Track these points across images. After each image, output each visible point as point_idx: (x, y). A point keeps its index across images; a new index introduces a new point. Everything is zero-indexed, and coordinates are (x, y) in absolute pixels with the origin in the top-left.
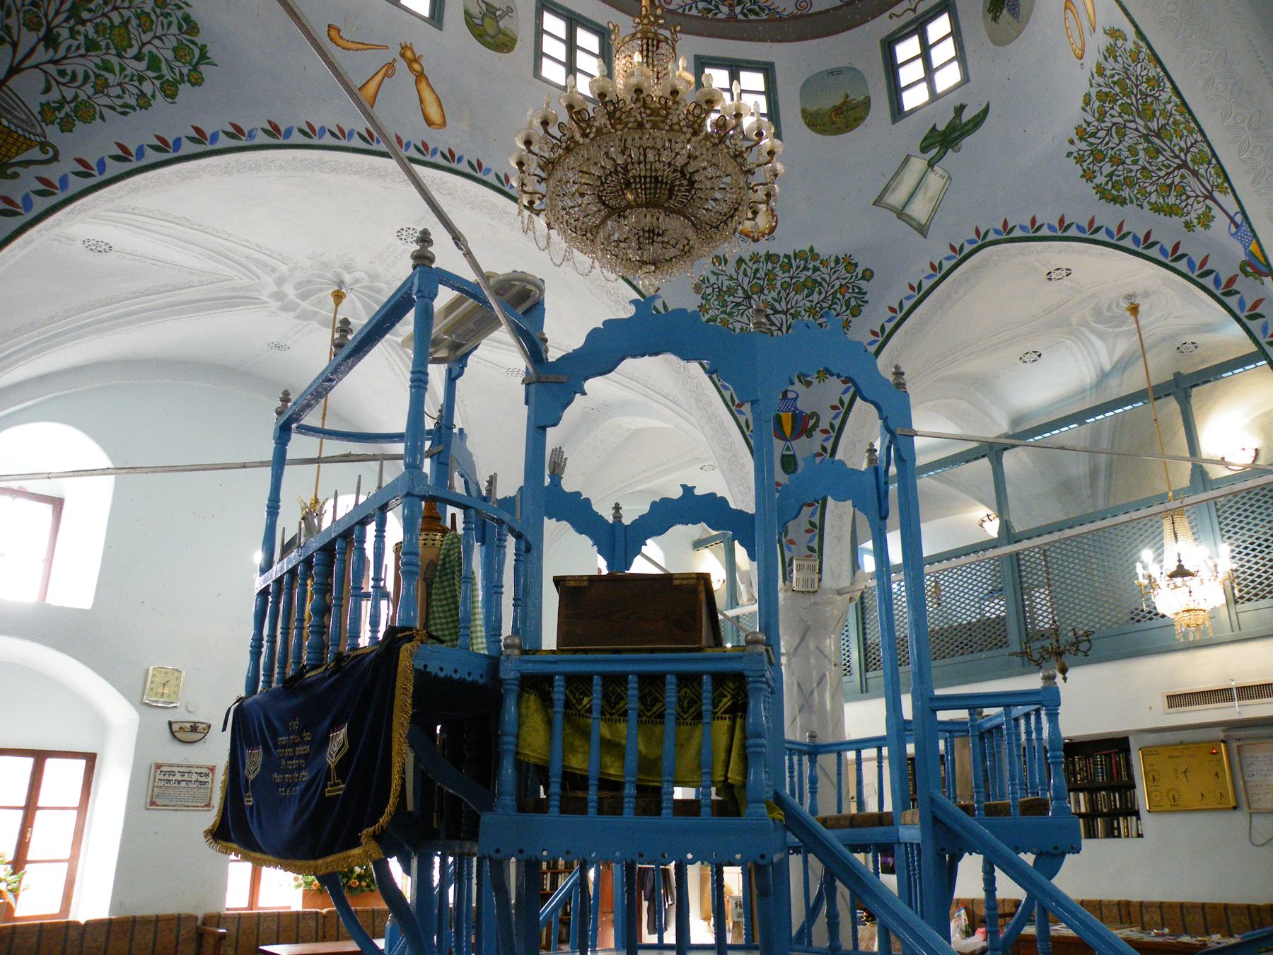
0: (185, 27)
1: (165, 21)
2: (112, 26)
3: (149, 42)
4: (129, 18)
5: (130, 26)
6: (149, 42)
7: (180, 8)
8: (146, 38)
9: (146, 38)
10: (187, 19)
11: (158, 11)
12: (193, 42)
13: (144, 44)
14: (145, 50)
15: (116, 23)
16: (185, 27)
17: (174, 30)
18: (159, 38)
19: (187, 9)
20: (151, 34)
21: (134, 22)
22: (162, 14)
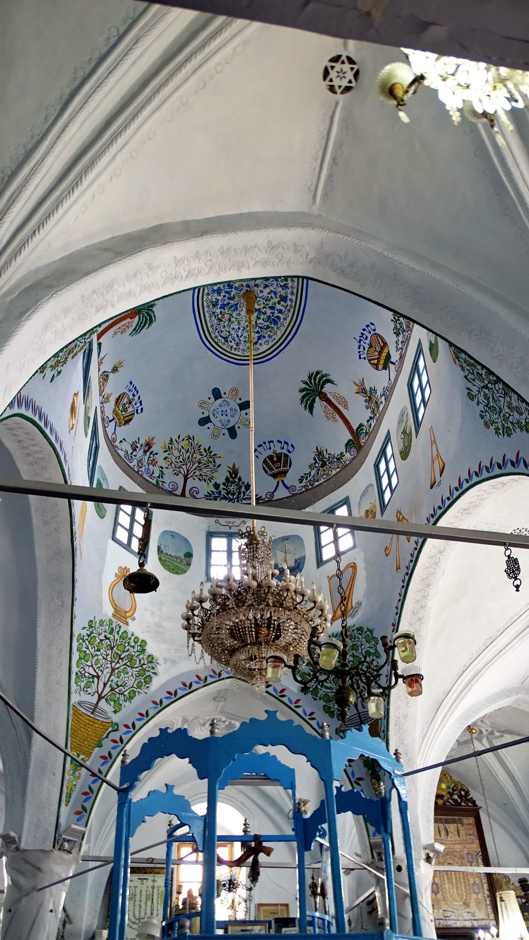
0: (360, 632)
1: (357, 639)
2: (353, 661)
3: (362, 650)
4: (352, 653)
5: (355, 655)
6: (362, 650)
7: (353, 630)
8: (360, 651)
9: (360, 651)
10: (358, 629)
11: (353, 640)
12: (366, 632)
13: (362, 653)
14: (364, 654)
15: (352, 659)
16: (360, 632)
17: (360, 637)
18: (362, 645)
19: (355, 628)
20: (360, 648)
21: (354, 652)
22: (354, 639)
